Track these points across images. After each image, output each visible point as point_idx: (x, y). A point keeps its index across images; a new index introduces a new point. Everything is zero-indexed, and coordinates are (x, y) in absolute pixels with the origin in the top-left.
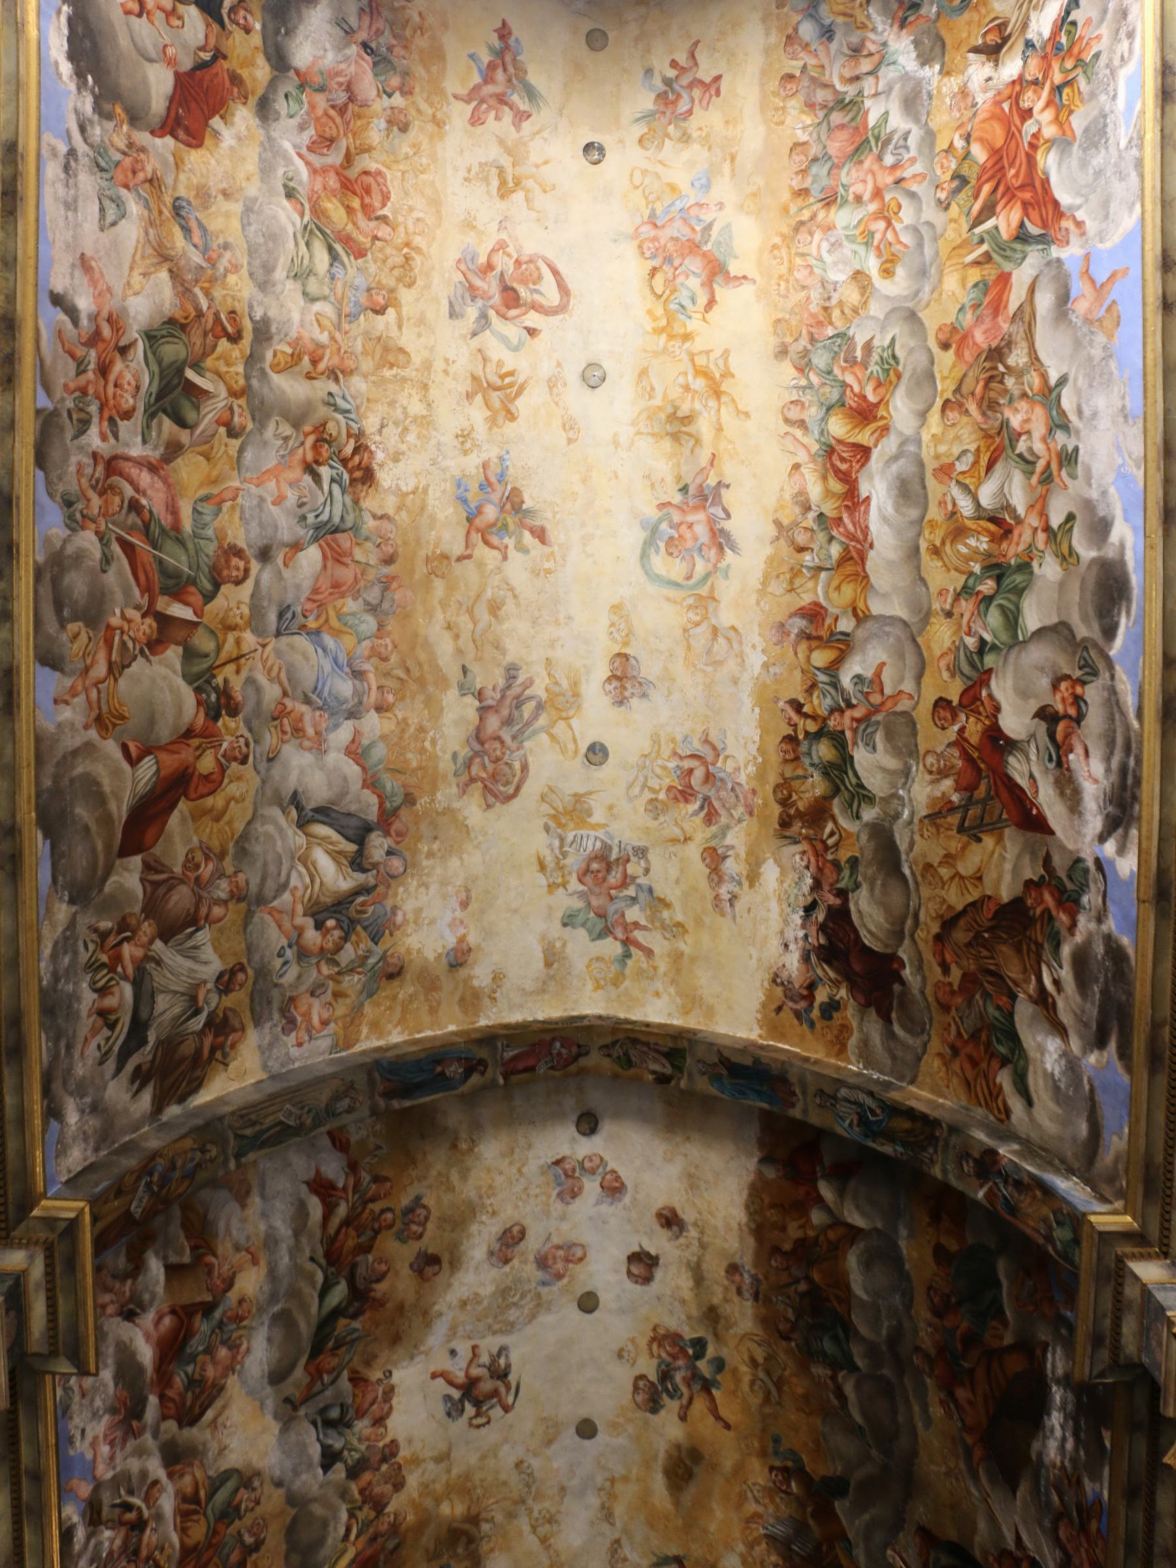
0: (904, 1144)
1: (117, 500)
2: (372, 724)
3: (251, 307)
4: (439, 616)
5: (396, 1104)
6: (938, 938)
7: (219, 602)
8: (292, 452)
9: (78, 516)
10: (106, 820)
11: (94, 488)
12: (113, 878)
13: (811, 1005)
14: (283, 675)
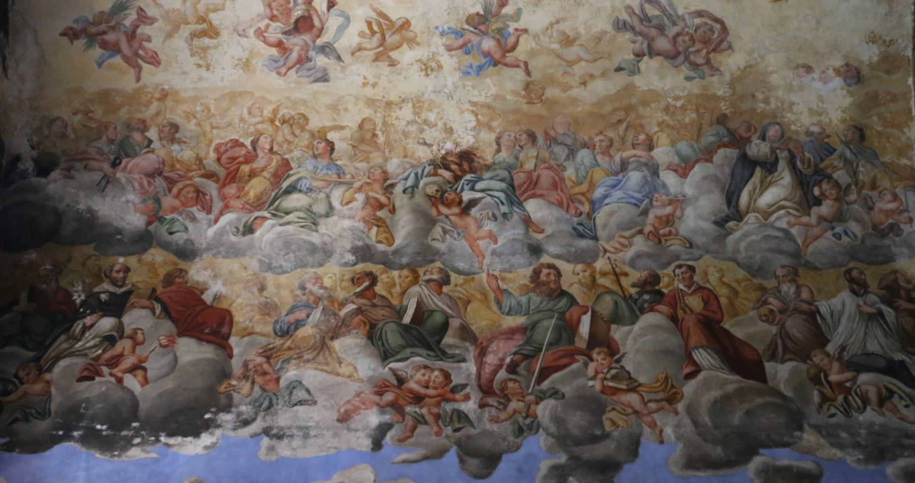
1: (510, 384)
2: (662, 154)
3: (346, 264)
4: (575, 92)
7: (575, 291)
8: (455, 226)
9: (528, 421)
10: (741, 393)
11: (505, 407)
12: (782, 388)
14: (627, 234)
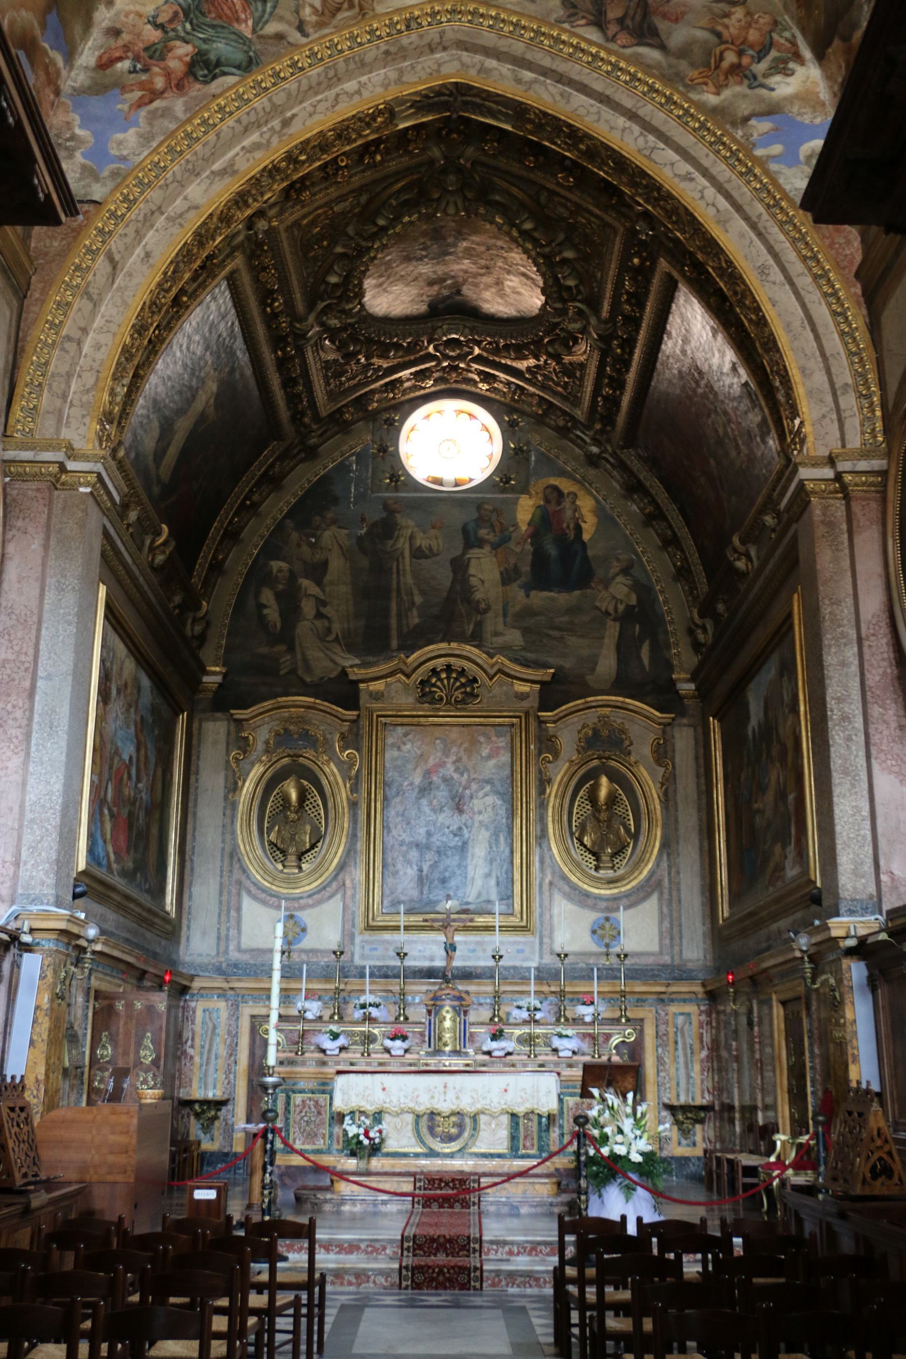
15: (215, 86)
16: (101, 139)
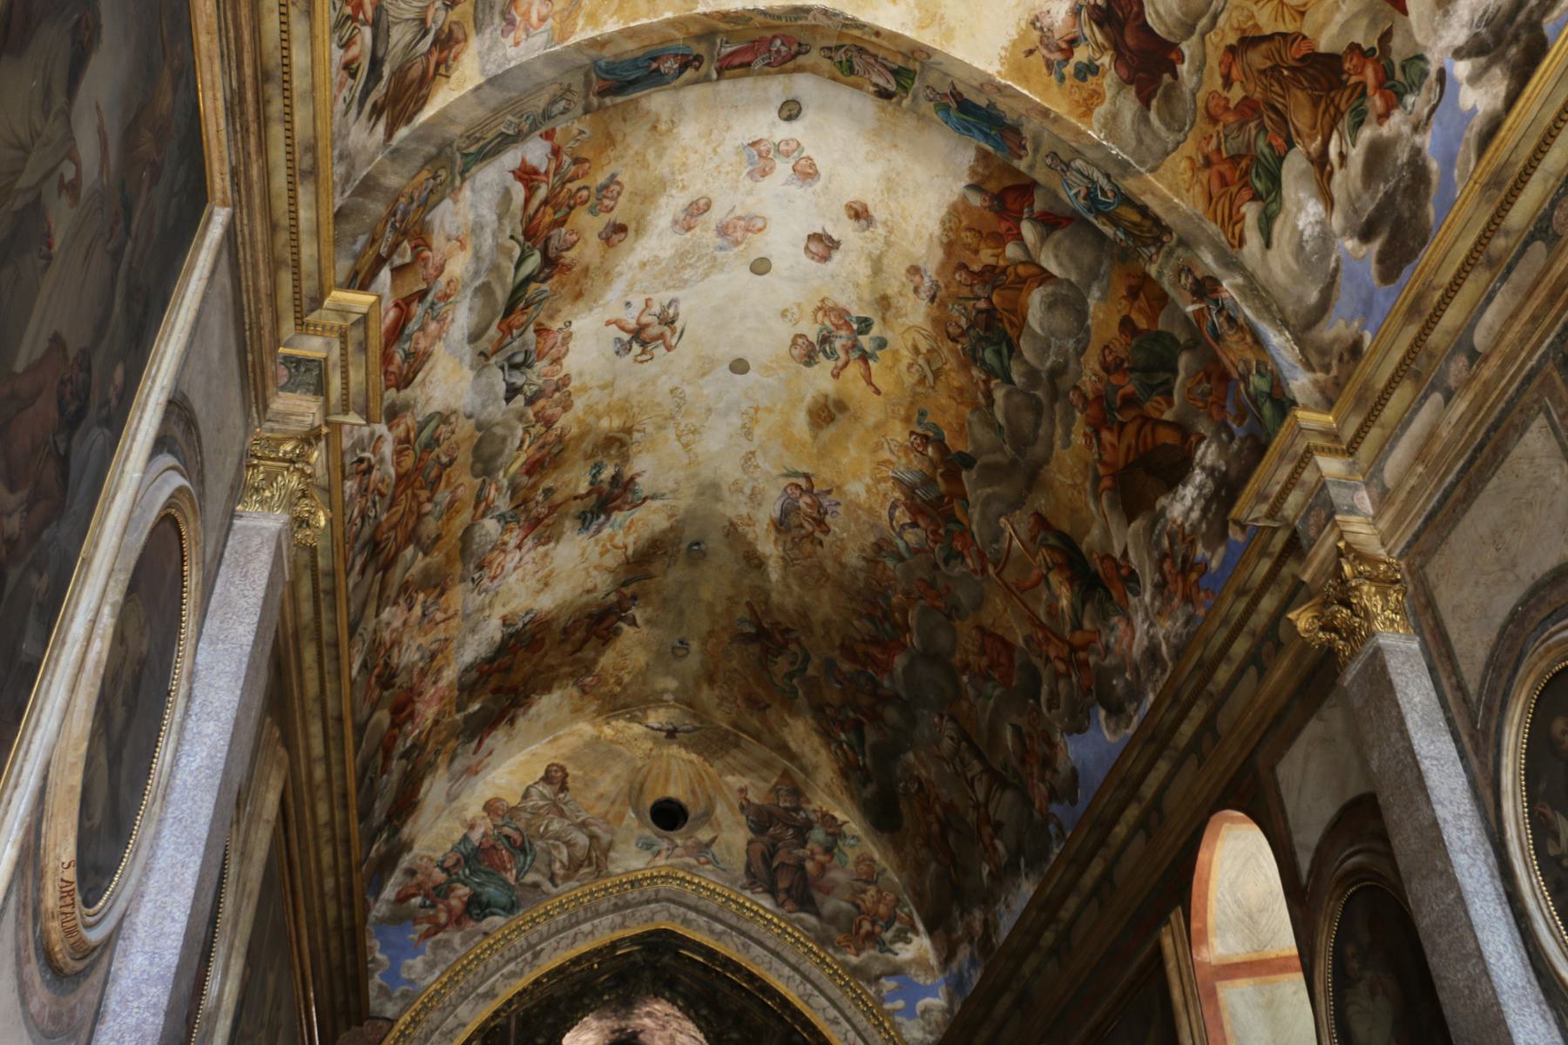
0: (1126, 233)
5: (608, 101)
6: (1231, 49)
13: (1067, 60)
15: (485, 924)
16: (396, 962)
